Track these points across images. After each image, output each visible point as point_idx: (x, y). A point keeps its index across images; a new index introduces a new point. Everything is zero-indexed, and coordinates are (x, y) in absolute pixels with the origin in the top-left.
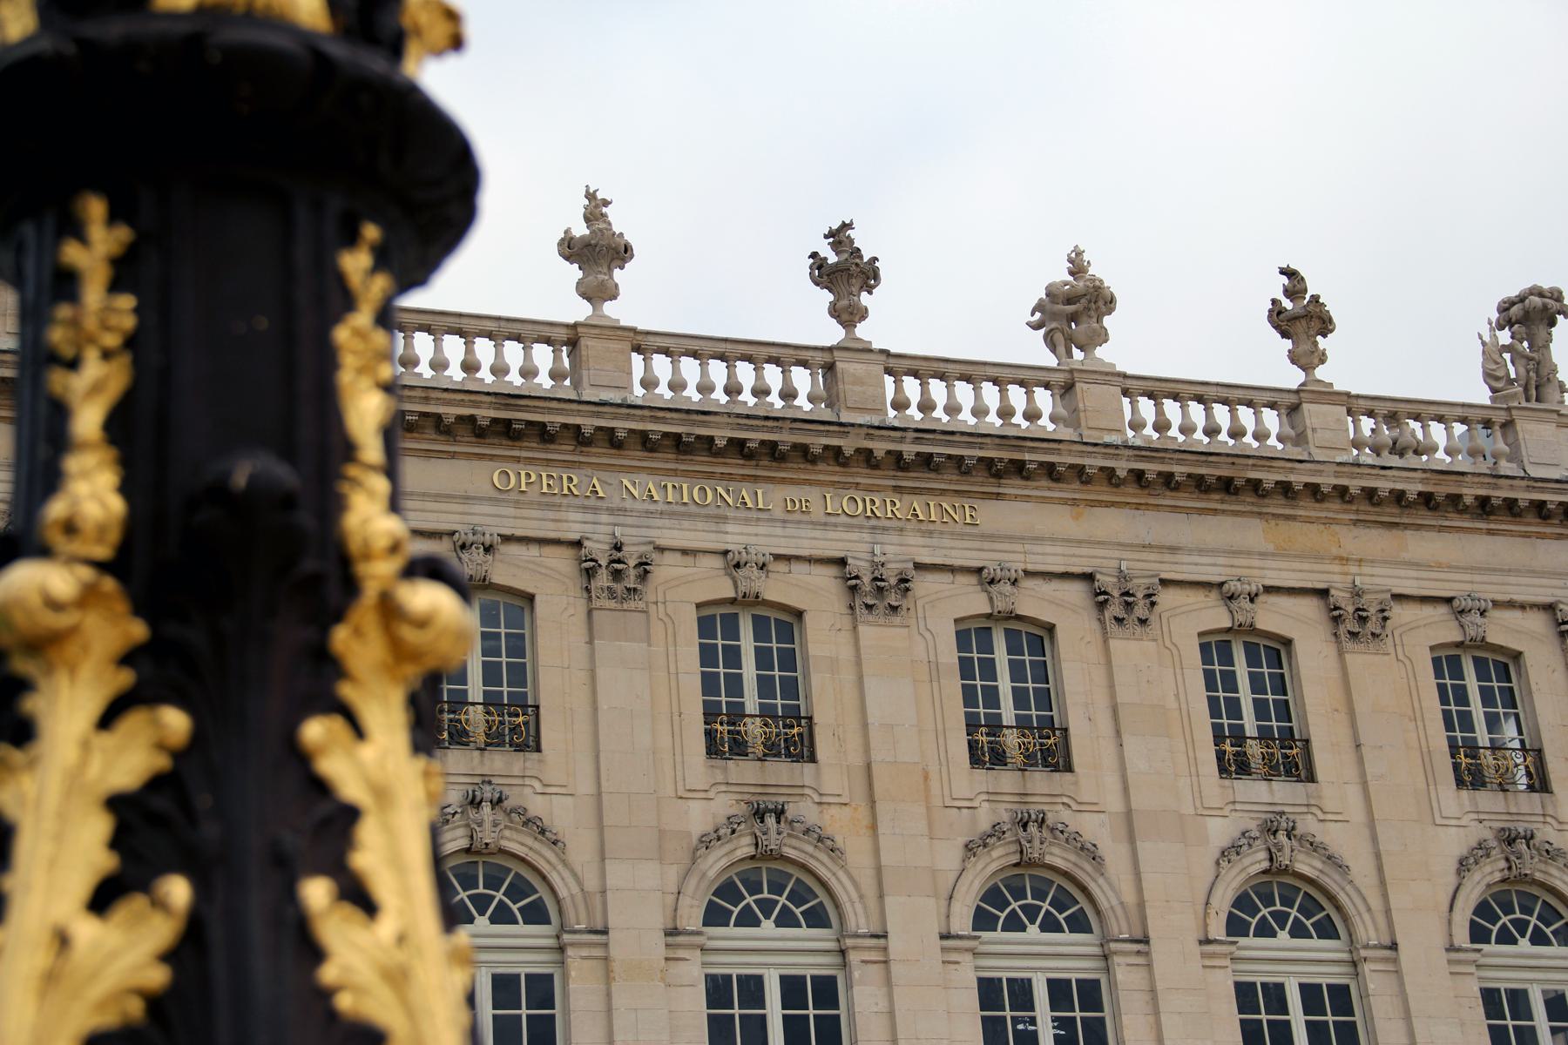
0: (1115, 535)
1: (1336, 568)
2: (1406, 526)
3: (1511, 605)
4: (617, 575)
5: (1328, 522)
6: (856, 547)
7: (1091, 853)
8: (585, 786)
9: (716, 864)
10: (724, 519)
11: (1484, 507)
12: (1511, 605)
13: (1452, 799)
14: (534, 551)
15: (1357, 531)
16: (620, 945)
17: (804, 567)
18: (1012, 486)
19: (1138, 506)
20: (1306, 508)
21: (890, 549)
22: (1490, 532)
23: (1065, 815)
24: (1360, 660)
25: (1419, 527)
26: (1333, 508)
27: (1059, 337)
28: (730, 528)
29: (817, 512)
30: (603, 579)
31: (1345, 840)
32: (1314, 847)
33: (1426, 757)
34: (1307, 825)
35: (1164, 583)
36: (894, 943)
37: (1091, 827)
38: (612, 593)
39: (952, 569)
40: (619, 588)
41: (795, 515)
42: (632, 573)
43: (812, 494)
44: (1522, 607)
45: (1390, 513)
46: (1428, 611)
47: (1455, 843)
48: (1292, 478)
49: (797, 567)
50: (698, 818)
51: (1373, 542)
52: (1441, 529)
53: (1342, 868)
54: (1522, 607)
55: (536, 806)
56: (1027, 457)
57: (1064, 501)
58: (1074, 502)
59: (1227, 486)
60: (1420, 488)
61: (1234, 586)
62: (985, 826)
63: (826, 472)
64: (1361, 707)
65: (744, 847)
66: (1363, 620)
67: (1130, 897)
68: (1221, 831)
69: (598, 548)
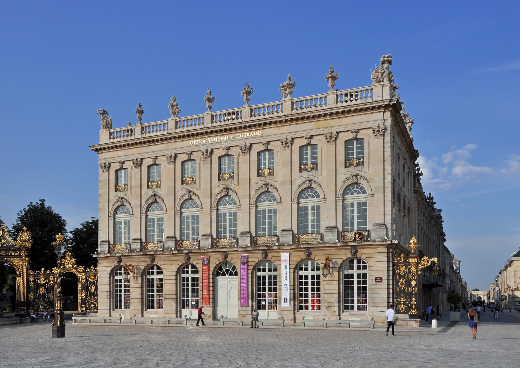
4: (206, 155)
10: (221, 142)
23: (272, 183)
28: (223, 143)
30: (205, 156)
36: (242, 206)
37: (276, 184)
38: (206, 158)
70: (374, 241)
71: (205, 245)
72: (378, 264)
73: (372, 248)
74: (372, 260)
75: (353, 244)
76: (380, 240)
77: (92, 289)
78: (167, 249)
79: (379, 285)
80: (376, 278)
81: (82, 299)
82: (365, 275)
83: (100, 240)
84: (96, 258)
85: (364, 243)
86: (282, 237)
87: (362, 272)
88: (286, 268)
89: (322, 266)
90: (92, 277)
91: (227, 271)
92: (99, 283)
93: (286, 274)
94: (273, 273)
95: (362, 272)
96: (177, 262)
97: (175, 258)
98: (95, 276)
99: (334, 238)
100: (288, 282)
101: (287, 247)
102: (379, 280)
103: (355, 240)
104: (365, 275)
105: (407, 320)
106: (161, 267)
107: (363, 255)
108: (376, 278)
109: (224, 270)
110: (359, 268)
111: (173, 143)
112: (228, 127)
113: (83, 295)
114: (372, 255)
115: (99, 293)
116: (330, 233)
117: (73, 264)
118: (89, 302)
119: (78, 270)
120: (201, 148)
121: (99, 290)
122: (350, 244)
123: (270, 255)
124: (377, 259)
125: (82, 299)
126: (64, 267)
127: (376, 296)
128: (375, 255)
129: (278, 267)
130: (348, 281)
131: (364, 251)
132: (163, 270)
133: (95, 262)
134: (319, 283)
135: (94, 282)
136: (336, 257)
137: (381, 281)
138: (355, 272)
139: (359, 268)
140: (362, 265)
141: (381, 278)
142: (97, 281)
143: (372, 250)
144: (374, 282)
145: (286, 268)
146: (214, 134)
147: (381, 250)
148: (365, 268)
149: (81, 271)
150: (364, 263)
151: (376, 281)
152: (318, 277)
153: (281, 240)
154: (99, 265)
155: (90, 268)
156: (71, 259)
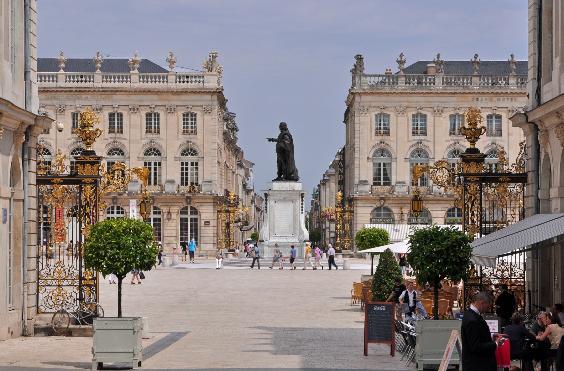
0: (134, 99)
4: (60, 110)
7: (123, 146)
8: (55, 138)
9: (72, 148)
11: (192, 92)
13: (181, 136)
14: (50, 107)
26: (168, 93)
29: (89, 98)
31: (163, 143)
32: (157, 144)
33: (178, 130)
34: (158, 141)
37: (125, 143)
41: (86, 99)
43: (89, 96)
46: (183, 107)
47: (180, 142)
50: (70, 142)
51: (176, 97)
53: (161, 147)
55: (49, 141)
62: (109, 142)
65: (75, 146)
67: (128, 151)
68: (144, 142)
70: (204, 194)
72: (206, 211)
74: (203, 208)
75: (188, 195)
76: (209, 193)
79: (207, 228)
80: (205, 222)
82: (196, 219)
87: (194, 216)
88: (133, 212)
95: (194, 216)
101: (135, 196)
102: (207, 223)
103: (190, 192)
104: (196, 219)
108: (205, 222)
110: (191, 213)
112: (83, 90)
120: (55, 102)
122: (186, 195)
123: (119, 201)
127: (206, 235)
128: (205, 204)
130: (183, 222)
136: (176, 204)
138: (189, 216)
139: (191, 213)
140: (195, 211)
141: (209, 222)
143: (203, 201)
144: (203, 225)
145: (133, 212)
147: (209, 201)
148: (196, 213)
150: (195, 209)
153: (129, 189)
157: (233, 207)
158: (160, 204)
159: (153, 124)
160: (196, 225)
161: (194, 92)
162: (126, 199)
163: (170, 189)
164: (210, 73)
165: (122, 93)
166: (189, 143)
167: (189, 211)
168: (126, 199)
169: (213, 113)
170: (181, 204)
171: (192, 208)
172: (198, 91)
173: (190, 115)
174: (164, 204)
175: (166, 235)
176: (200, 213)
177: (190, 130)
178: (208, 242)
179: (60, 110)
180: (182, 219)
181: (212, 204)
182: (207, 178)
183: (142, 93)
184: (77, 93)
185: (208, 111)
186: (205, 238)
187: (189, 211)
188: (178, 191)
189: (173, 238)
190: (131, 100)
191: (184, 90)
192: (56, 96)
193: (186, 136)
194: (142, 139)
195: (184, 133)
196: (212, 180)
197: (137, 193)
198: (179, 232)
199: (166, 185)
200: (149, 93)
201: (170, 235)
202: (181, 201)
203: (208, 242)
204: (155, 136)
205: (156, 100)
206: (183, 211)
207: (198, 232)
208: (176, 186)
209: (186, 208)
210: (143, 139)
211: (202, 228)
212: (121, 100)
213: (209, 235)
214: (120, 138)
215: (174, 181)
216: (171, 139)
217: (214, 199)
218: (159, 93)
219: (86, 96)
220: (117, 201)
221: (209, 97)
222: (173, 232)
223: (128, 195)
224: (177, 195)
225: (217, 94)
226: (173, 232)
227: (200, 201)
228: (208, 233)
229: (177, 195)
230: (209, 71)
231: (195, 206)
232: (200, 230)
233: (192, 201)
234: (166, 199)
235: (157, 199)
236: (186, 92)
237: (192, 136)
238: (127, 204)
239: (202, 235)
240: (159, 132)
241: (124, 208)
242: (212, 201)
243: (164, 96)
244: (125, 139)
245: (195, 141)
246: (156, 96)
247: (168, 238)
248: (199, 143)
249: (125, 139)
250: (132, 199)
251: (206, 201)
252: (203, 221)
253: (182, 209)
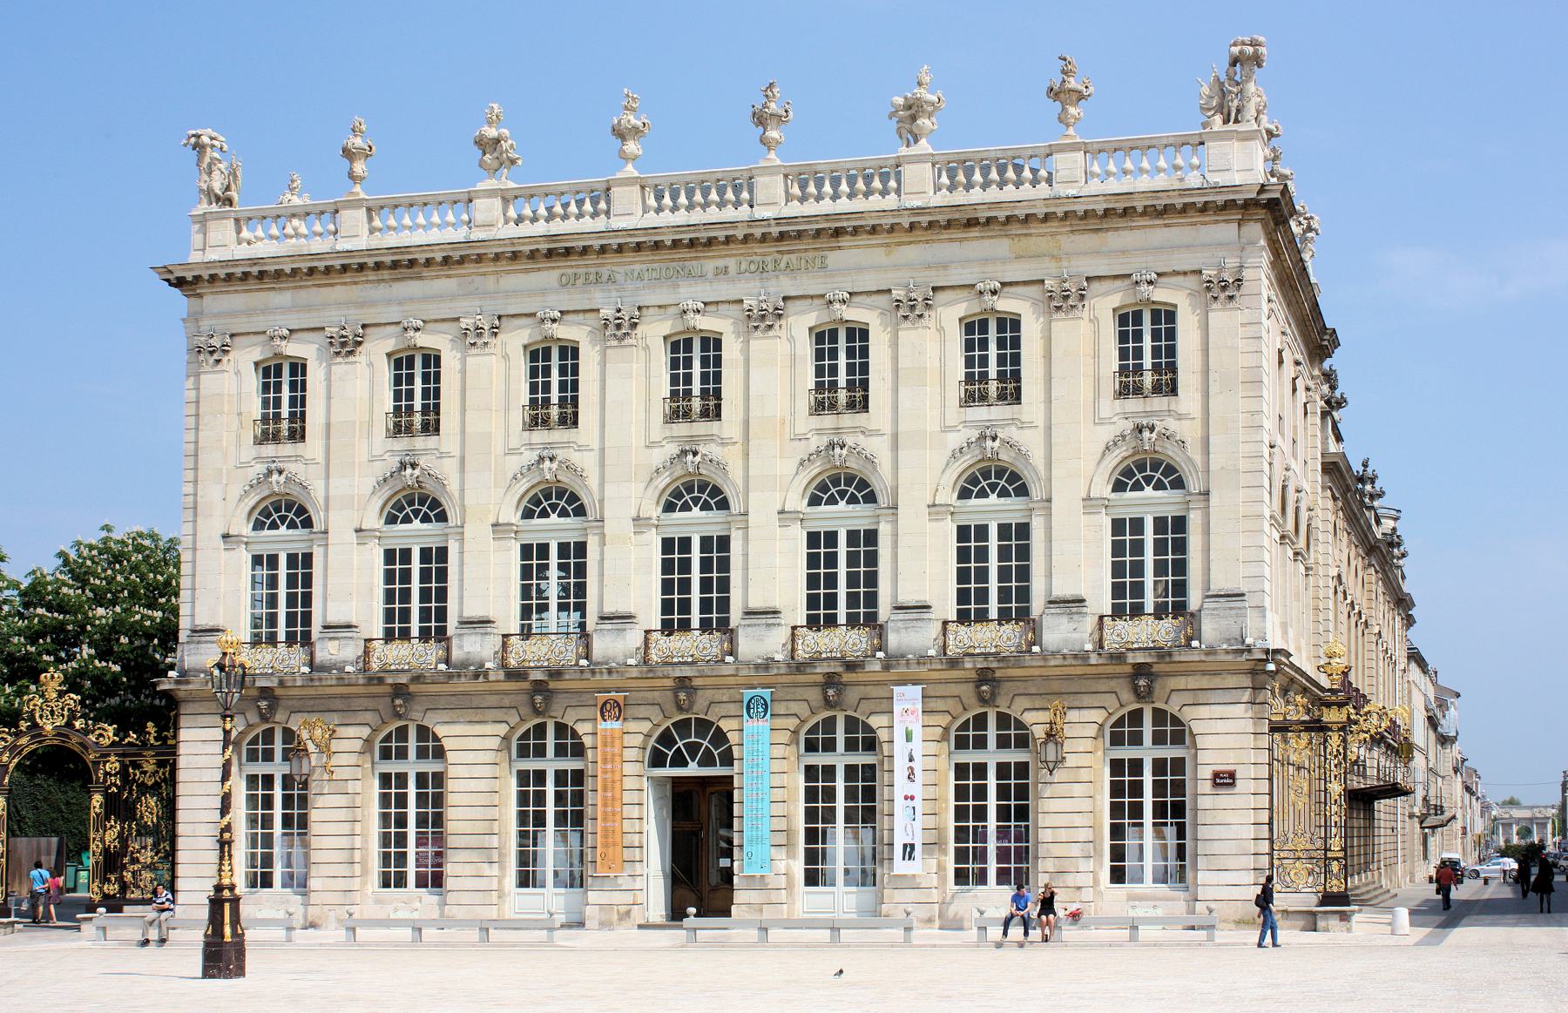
1: (1053, 264)
2: (1108, 230)
3: (1176, 273)
5: (1053, 235)
6: (753, 292)
8: (596, 446)
12: (1176, 273)
14: (581, 316)
15: (1073, 237)
16: (609, 528)
17: (726, 306)
18: (845, 241)
19: (927, 242)
20: (1035, 228)
21: (771, 290)
22: (1166, 226)
24: (1061, 325)
25: (1117, 229)
26: (1053, 226)
27: (904, 132)
30: (611, 330)
35: (934, 289)
39: (812, 297)
40: (619, 333)
42: (626, 324)
43: (731, 263)
44: (1185, 273)
45: (1093, 223)
46: (1118, 283)
47: (1107, 434)
48: (1016, 212)
49: (721, 307)
52: (1131, 228)
54: (1185, 273)
56: (845, 224)
57: (882, 245)
58: (887, 245)
59: (971, 223)
60: (1105, 206)
61: (980, 286)
62: (813, 449)
63: (734, 248)
64: (1056, 353)
66: (1066, 298)
68: (955, 440)
69: (608, 312)
70: (1211, 651)
71: (610, 653)
72: (1220, 726)
73: (1204, 673)
74: (1203, 711)
77: (149, 809)
78: (464, 665)
79: (1225, 799)
80: (1216, 775)
81: (106, 851)
82: (1179, 765)
83: (184, 624)
84: (166, 694)
85: (1177, 658)
86: (898, 631)
87: (1169, 752)
88: (909, 737)
89: (1039, 732)
90: (149, 767)
91: (693, 749)
92: (181, 789)
93: (911, 760)
94: (861, 759)
95: (1169, 752)
96: (499, 714)
97: (492, 700)
98: (161, 764)
99: (1076, 636)
100: (916, 789)
101: (914, 669)
102: (1224, 780)
104: (1179, 765)
105: (1314, 914)
106: (440, 731)
107: (1174, 696)
108: (1216, 775)
109: (680, 744)
111: (492, 278)
112: (703, 235)
113: (111, 836)
114: (1202, 697)
115: (181, 829)
116: (1064, 619)
117: (73, 716)
118: (135, 861)
119: (92, 738)
121: (181, 816)
123: (852, 695)
124: (1218, 711)
125: (106, 851)
126: (35, 725)
129: (882, 735)
131: (1181, 682)
132: (447, 744)
133: (167, 713)
134: (1023, 792)
135: (157, 786)
136: (1087, 700)
137: (1233, 785)
138: (1148, 753)
139: (1159, 739)
140: (1174, 730)
141: (1232, 775)
142: (172, 781)
143: (1204, 682)
144: (1205, 787)
145: (909, 737)
146: (646, 256)
147: (1231, 681)
148: (1178, 738)
149: (105, 742)
150: (1176, 721)
151: (1216, 785)
152: (1022, 769)
153: (893, 640)
154: (183, 721)
155: (141, 731)
156: (61, 694)
157: (1341, 705)
158: (1022, 703)
159: (994, 361)
160: (1179, 787)
161: (1162, 211)
162: (878, 683)
163: (1060, 633)
164: (1231, 126)
165: (863, 240)
166: (1146, 434)
167: (1148, 729)
168: (878, 683)
169: (1245, 301)
170: (1111, 701)
171: (1160, 716)
172: (1179, 202)
173: (1147, 318)
174: (1038, 703)
175: (1045, 835)
176: (1193, 735)
177: (1148, 379)
178: (1232, 863)
179: (619, 326)
180: (1116, 766)
181: (1246, 696)
182: (1219, 583)
183: (945, 235)
184: (684, 253)
185: (1225, 289)
186: (1216, 848)
187: (1148, 729)
188: (1100, 644)
189: (1075, 850)
190: (896, 267)
191: (1120, 206)
192: (605, 272)
193: (1133, 404)
194: (946, 429)
195: (1124, 392)
196: (1243, 589)
197: (922, 659)
198: (1107, 822)
199: (1047, 621)
200: (975, 232)
201: (1063, 835)
202: (1113, 684)
203: (1232, 863)
204: (999, 412)
205: (1004, 261)
206: (1123, 731)
207: (1187, 820)
208: (1090, 623)
209: (1136, 717)
210: (952, 429)
211: (1203, 802)
212: (860, 269)
213: (1232, 832)
214: (855, 430)
215: (1080, 601)
216: (1071, 416)
217: (1253, 673)
218: (1015, 229)
219: (721, 263)
220: (839, 693)
221: (1225, 231)
222: (1078, 820)
223: (887, 667)
224: (1094, 659)
225: (1262, 214)
226: (1078, 820)
227: (1192, 682)
228: (1230, 826)
229: (1094, 659)
230: (1226, 121)
231: (1173, 708)
232: (1195, 810)
233: (1157, 685)
234: (1047, 678)
235: (1010, 679)
236: (1127, 212)
237: (1159, 403)
238: (885, 705)
239: (1203, 832)
240: (1016, 397)
241: (874, 721)
242: (1246, 681)
243: (1038, 239)
244: (876, 433)
245: (1172, 425)
246: (1006, 242)
247: (1057, 850)
248: (1188, 431)
249: (876, 433)
250: (902, 682)
251: (1216, 682)
252: (1206, 773)
253: (1119, 723)
